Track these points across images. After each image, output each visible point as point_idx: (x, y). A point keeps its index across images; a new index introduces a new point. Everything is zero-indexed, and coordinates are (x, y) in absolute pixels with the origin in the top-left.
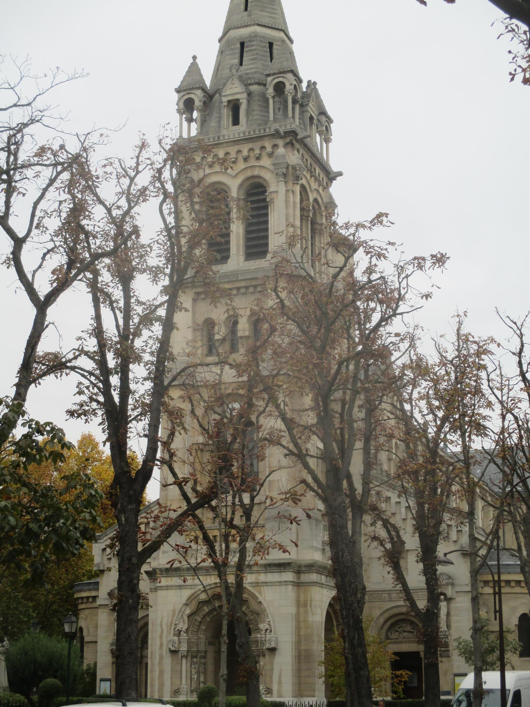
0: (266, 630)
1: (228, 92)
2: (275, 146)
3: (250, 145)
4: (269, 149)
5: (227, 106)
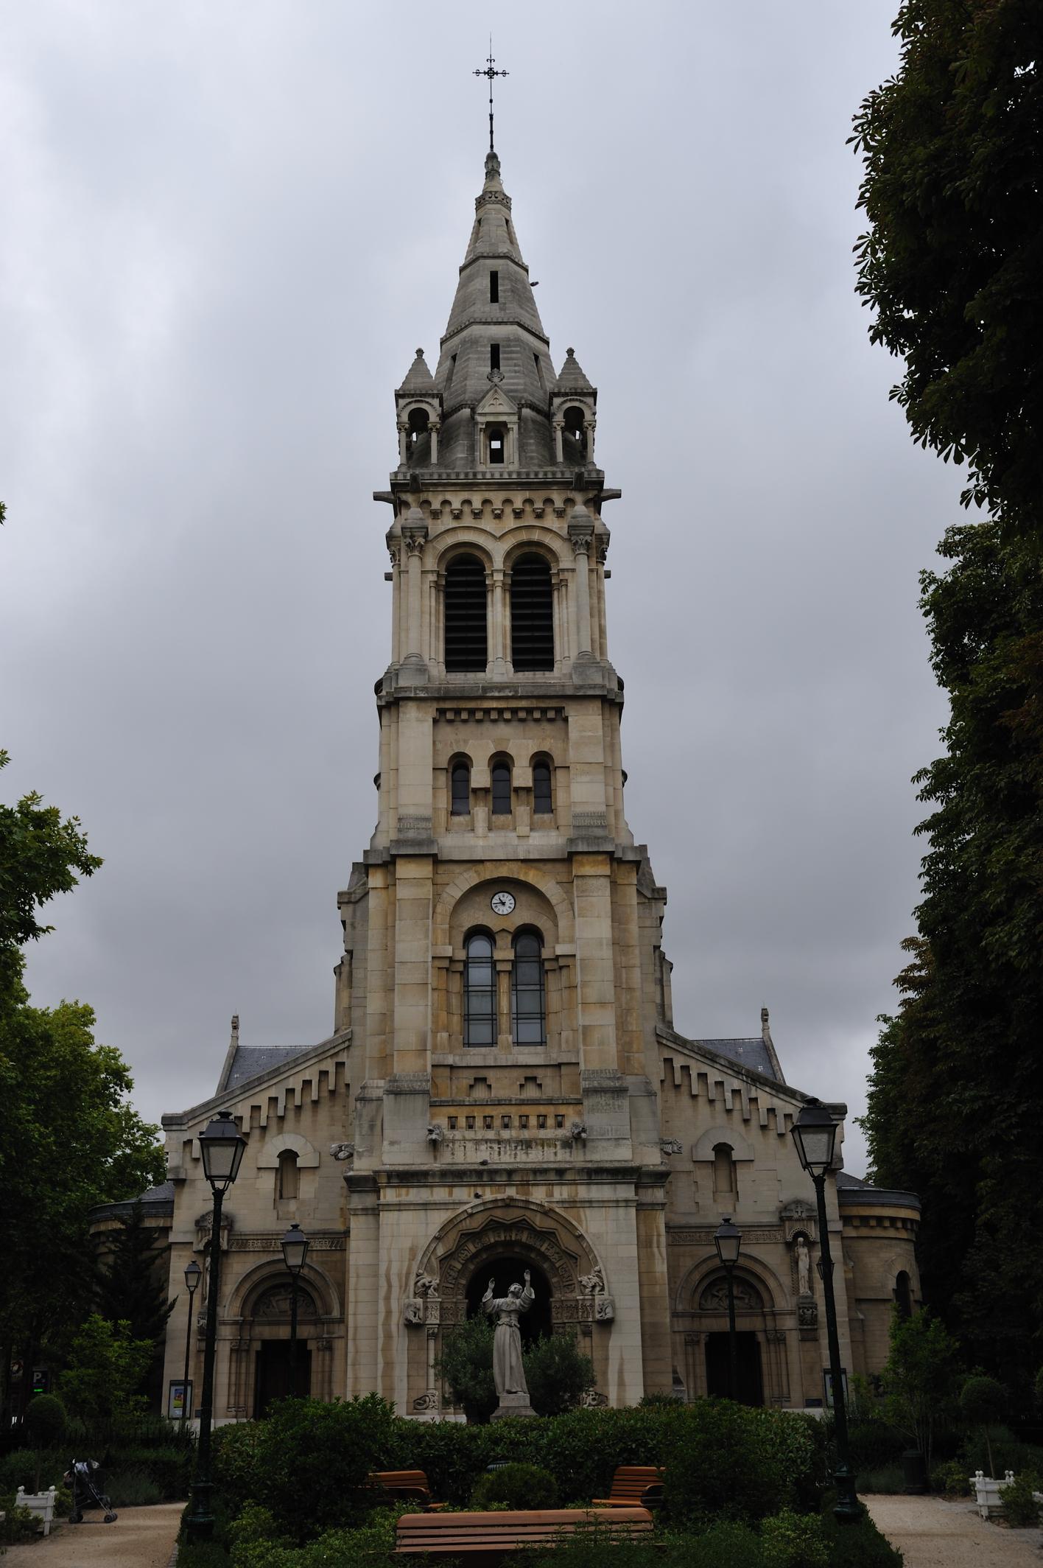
0: (594, 1287)
1: (487, 410)
2: (570, 502)
3: (527, 494)
4: (559, 504)
5: (485, 430)
